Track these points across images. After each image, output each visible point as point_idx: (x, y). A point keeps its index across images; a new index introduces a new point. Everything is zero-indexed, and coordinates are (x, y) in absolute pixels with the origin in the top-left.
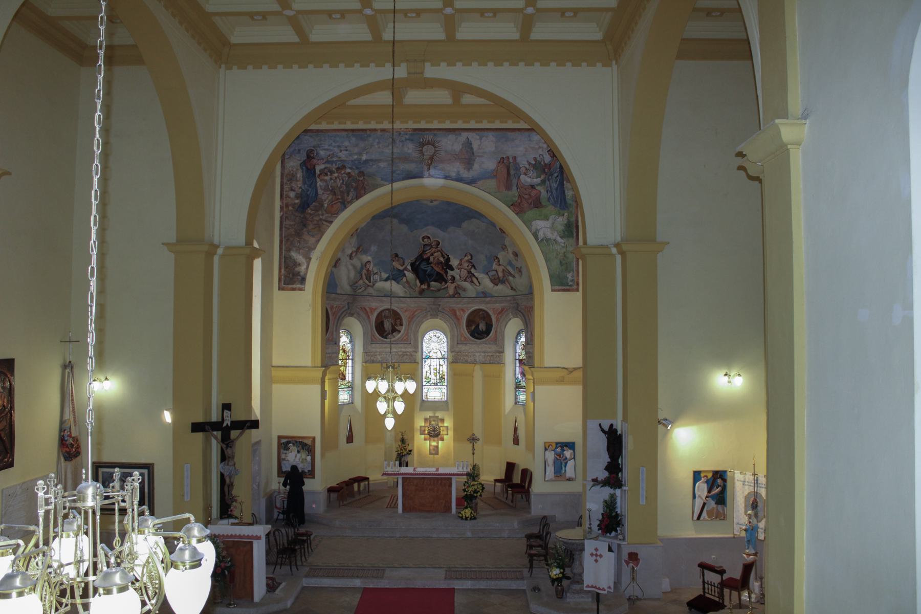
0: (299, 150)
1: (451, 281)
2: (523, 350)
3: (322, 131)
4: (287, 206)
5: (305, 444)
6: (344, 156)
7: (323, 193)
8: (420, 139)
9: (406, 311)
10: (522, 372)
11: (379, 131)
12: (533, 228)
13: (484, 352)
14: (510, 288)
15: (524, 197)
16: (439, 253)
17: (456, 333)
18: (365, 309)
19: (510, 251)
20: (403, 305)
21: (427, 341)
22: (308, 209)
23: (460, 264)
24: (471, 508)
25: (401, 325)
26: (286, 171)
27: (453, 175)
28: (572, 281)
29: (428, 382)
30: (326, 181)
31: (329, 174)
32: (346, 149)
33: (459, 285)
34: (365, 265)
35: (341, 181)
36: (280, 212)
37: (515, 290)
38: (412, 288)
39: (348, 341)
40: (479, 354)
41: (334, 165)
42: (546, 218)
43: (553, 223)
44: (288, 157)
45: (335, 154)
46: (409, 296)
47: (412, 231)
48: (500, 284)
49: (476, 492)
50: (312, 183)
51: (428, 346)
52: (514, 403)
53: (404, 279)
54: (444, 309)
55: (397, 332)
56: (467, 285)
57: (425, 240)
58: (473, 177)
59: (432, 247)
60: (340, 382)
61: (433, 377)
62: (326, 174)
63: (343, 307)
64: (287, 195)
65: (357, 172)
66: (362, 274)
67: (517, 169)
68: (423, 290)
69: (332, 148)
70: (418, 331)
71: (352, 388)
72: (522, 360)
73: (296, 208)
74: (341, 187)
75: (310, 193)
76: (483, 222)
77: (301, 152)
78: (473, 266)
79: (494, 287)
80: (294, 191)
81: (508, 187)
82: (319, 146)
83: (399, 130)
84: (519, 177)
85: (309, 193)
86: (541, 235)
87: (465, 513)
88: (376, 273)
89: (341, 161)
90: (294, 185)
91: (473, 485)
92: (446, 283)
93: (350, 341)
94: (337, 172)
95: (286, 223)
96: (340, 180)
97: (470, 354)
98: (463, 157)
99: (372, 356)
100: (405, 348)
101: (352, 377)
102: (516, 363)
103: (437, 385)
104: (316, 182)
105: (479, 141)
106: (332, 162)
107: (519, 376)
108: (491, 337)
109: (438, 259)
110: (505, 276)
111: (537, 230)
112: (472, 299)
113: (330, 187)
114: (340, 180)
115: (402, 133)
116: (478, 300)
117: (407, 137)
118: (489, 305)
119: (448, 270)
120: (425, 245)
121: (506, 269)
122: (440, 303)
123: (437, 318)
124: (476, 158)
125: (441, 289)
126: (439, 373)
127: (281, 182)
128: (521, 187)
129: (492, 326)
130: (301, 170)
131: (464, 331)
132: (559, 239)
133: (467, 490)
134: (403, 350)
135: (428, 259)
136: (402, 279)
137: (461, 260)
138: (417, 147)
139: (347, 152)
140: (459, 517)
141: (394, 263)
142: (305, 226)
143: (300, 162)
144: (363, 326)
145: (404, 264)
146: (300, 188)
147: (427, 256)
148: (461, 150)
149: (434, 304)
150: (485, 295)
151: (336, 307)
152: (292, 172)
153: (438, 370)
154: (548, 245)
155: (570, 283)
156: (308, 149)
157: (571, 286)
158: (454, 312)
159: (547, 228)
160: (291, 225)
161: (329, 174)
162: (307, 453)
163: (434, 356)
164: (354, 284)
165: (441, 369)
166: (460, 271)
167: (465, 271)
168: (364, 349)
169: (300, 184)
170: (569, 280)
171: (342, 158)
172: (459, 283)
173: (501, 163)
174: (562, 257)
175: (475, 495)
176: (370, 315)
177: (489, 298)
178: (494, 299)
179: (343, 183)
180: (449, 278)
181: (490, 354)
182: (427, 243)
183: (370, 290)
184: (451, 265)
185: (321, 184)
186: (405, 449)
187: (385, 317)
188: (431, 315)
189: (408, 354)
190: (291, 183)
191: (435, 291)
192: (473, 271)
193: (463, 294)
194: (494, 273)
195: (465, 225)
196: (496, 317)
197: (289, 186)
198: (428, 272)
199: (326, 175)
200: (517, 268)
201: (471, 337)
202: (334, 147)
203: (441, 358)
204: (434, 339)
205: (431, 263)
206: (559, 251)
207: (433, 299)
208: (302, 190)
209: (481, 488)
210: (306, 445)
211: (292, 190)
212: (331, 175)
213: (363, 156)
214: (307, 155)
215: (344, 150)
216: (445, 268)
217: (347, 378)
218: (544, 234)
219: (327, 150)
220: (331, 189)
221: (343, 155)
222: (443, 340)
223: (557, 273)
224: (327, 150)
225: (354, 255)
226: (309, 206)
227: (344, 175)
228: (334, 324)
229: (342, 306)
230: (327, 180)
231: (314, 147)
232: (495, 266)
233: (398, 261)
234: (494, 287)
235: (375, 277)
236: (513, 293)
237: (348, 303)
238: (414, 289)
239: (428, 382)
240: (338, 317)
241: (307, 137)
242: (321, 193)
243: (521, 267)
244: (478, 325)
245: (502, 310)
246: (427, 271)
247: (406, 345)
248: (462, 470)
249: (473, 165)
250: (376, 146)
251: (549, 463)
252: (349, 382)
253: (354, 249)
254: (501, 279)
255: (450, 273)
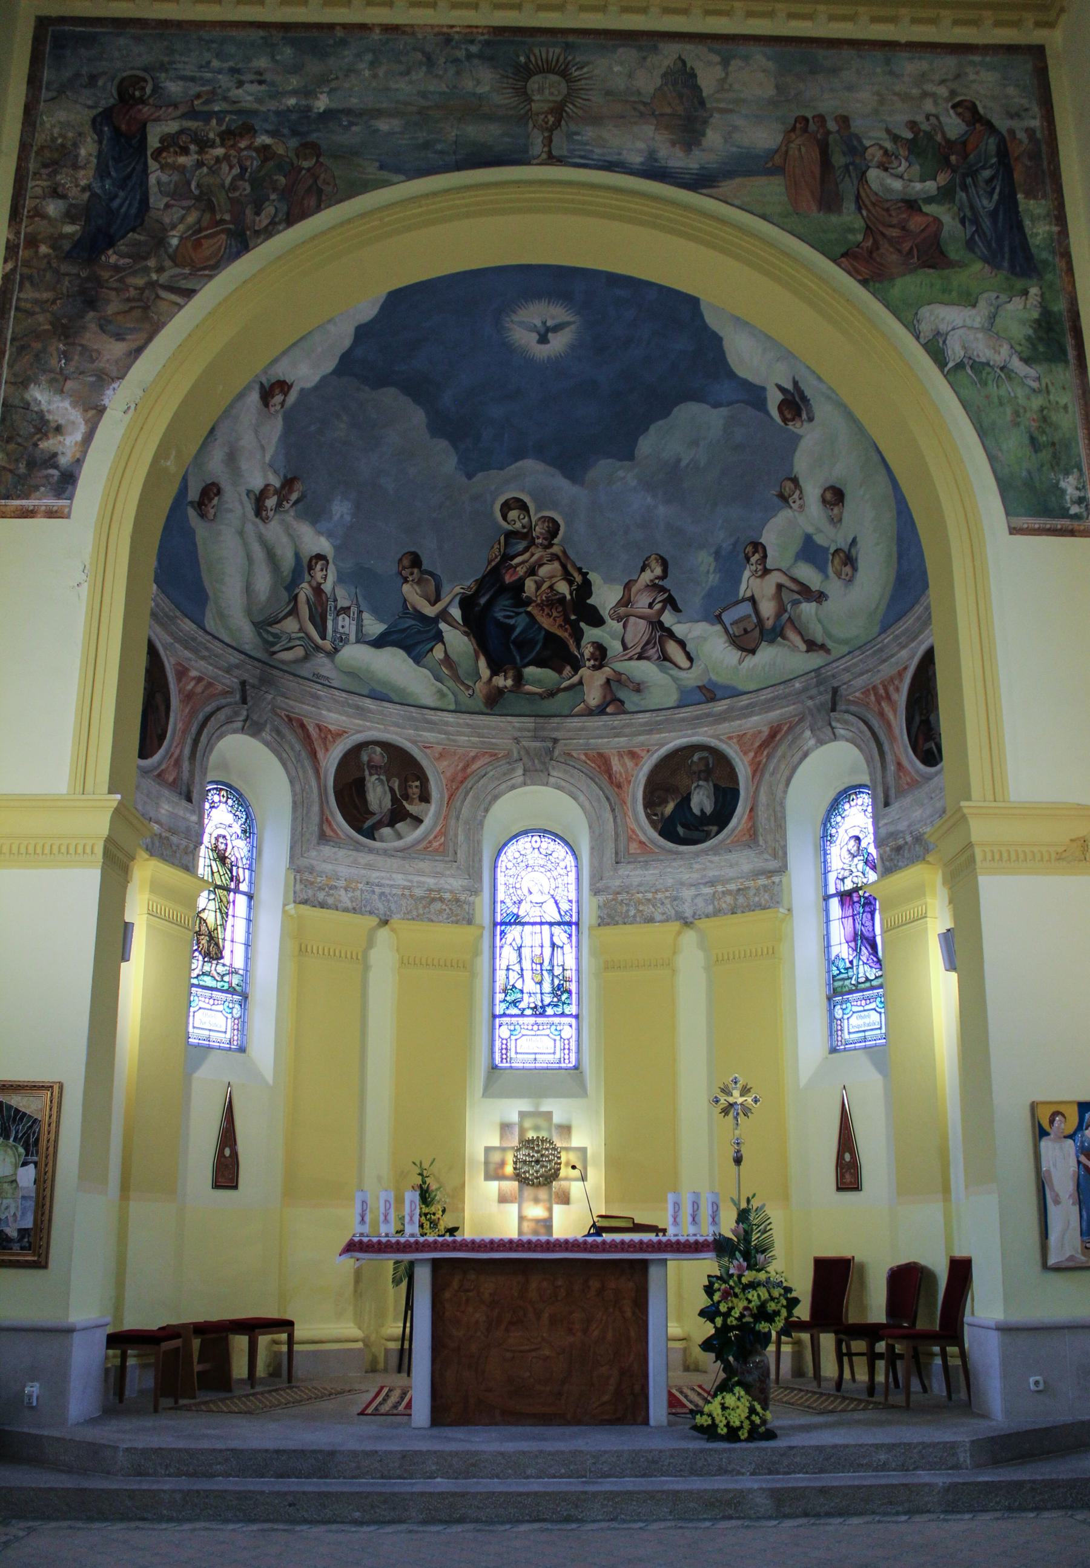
0: (93, 79)
1: (592, 662)
2: (854, 856)
3: (179, 24)
4: (32, 242)
5: (17, 1111)
6: (249, 98)
7: (167, 206)
8: (518, 56)
9: (442, 756)
10: (856, 934)
11: (378, 31)
12: (926, 328)
13: (712, 883)
14: (803, 647)
15: (883, 234)
16: (556, 565)
17: (610, 825)
18: (303, 726)
19: (812, 491)
20: (429, 736)
21: (510, 865)
22: (110, 252)
23: (626, 601)
24: (747, 1388)
25: (425, 798)
26: (40, 138)
27: (636, 159)
28: (1080, 501)
29: (514, 1003)
30: (182, 169)
31: (193, 147)
32: (259, 77)
33: (620, 674)
34: (310, 568)
35: (236, 171)
36: (6, 261)
37: (823, 647)
38: (463, 683)
39: (237, 828)
40: (692, 891)
41: (214, 122)
42: (969, 300)
43: (993, 317)
44: (54, 94)
45: (219, 91)
46: (452, 707)
47: (470, 476)
48: (763, 643)
49: (763, 1314)
50: (129, 177)
51: (512, 881)
52: (826, 1047)
53: (438, 653)
54: (569, 755)
55: (409, 820)
56: (646, 670)
57: (513, 514)
58: (702, 168)
59: (532, 543)
60: (198, 964)
61: (530, 986)
62: (181, 147)
63: (225, 693)
64: (36, 207)
65: (293, 143)
66: (296, 595)
67: (855, 148)
68: (500, 691)
69: (209, 75)
70: (481, 824)
71: (245, 997)
72: (856, 889)
73: (67, 245)
74: (233, 187)
75: (121, 205)
76: (716, 405)
77: (100, 83)
78: (671, 602)
79: (740, 662)
80: (63, 197)
81: (829, 202)
82: (163, 68)
83: (445, 30)
84: (864, 173)
85: (115, 204)
86: (955, 351)
87: (724, 1408)
88: (346, 610)
89: (239, 112)
90: (63, 178)
91: (753, 1285)
92: (576, 669)
93: (244, 832)
94: (223, 145)
95: (22, 295)
96: (231, 167)
97: (659, 896)
98: (668, 110)
99: (321, 889)
100: (437, 875)
101: (247, 959)
102: (827, 911)
103: (542, 1014)
104: (145, 172)
105: (719, 68)
106: (207, 116)
107: (841, 949)
108: (733, 830)
109: (551, 587)
110: (786, 611)
111: (938, 333)
112: (669, 712)
113: (193, 186)
114: (231, 167)
115: (456, 37)
116: (686, 713)
117: (474, 49)
118: (724, 728)
119: (582, 625)
120: (510, 535)
121: (794, 580)
122: (555, 735)
123: (547, 784)
124: (711, 116)
125: (559, 690)
126: (551, 971)
127: (18, 169)
128: (874, 204)
129: (735, 793)
130: (96, 137)
131: (637, 820)
132: (1016, 364)
133: (723, 1308)
134: (431, 881)
135: (519, 585)
136: (431, 650)
137: (628, 586)
138: (507, 77)
139: (263, 87)
140: (700, 1429)
141: (406, 588)
142: (91, 303)
143: (95, 112)
144: (291, 782)
145: (438, 599)
146: (88, 188)
147: (514, 578)
148: (660, 89)
149: (535, 738)
150: (709, 693)
151: (199, 680)
152: (60, 141)
153: (546, 966)
154: (985, 384)
155: (1074, 510)
156: (125, 74)
157: (1077, 517)
158: (603, 763)
159: (971, 328)
160: (36, 302)
161: (193, 147)
162: (21, 1150)
163: (534, 914)
164: (271, 624)
165: (558, 959)
166: (625, 626)
167: (643, 623)
168: (292, 857)
169: (85, 177)
170: (1068, 497)
171: (243, 104)
172: (621, 666)
173: (798, 132)
174: (1034, 424)
175: (763, 1326)
176: (318, 749)
177: (728, 701)
178: (744, 701)
179: (241, 176)
180: (588, 651)
181: (732, 887)
182: (518, 525)
183: (322, 665)
184: (594, 609)
185: (165, 178)
186: (434, 1224)
187: (370, 767)
188: (525, 770)
189: (447, 896)
190: (55, 172)
191: (540, 695)
192: (668, 618)
193: (631, 700)
194: (746, 609)
195: (645, 445)
196: (751, 763)
197: (45, 184)
198: (518, 630)
199: (185, 151)
200: (837, 551)
201: (662, 841)
202: (220, 72)
203: (559, 924)
204: (534, 858)
205: (528, 602)
206: (1021, 401)
207: (532, 719)
208: (94, 195)
209: (784, 1302)
210: (19, 1116)
211: (56, 193)
212: (201, 151)
213: (318, 99)
214: (119, 93)
215: (252, 82)
216: (573, 617)
217: (226, 953)
218: (964, 348)
219: (192, 79)
220: (197, 192)
221: (247, 95)
222: (562, 864)
223: (1024, 474)
224: (192, 79)
225: (271, 502)
226: (111, 243)
227: (245, 153)
228: (185, 732)
229: (220, 687)
230: (184, 167)
231: (145, 70)
232: (749, 583)
233: (419, 582)
234: (740, 662)
235: (340, 623)
236: (816, 660)
237: (243, 684)
238: (468, 687)
239: (514, 1003)
240: (201, 717)
241: (122, 41)
242: (162, 206)
243: (854, 542)
244: (687, 799)
245: (773, 734)
246: (513, 628)
247: (440, 866)
248: (692, 1230)
249: (704, 135)
250: (367, 73)
251: (1058, 1187)
252: (233, 972)
253: (276, 482)
254: (769, 624)
255: (591, 634)
